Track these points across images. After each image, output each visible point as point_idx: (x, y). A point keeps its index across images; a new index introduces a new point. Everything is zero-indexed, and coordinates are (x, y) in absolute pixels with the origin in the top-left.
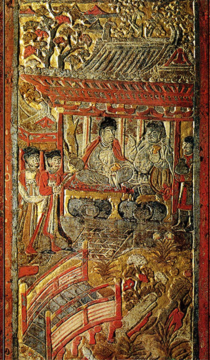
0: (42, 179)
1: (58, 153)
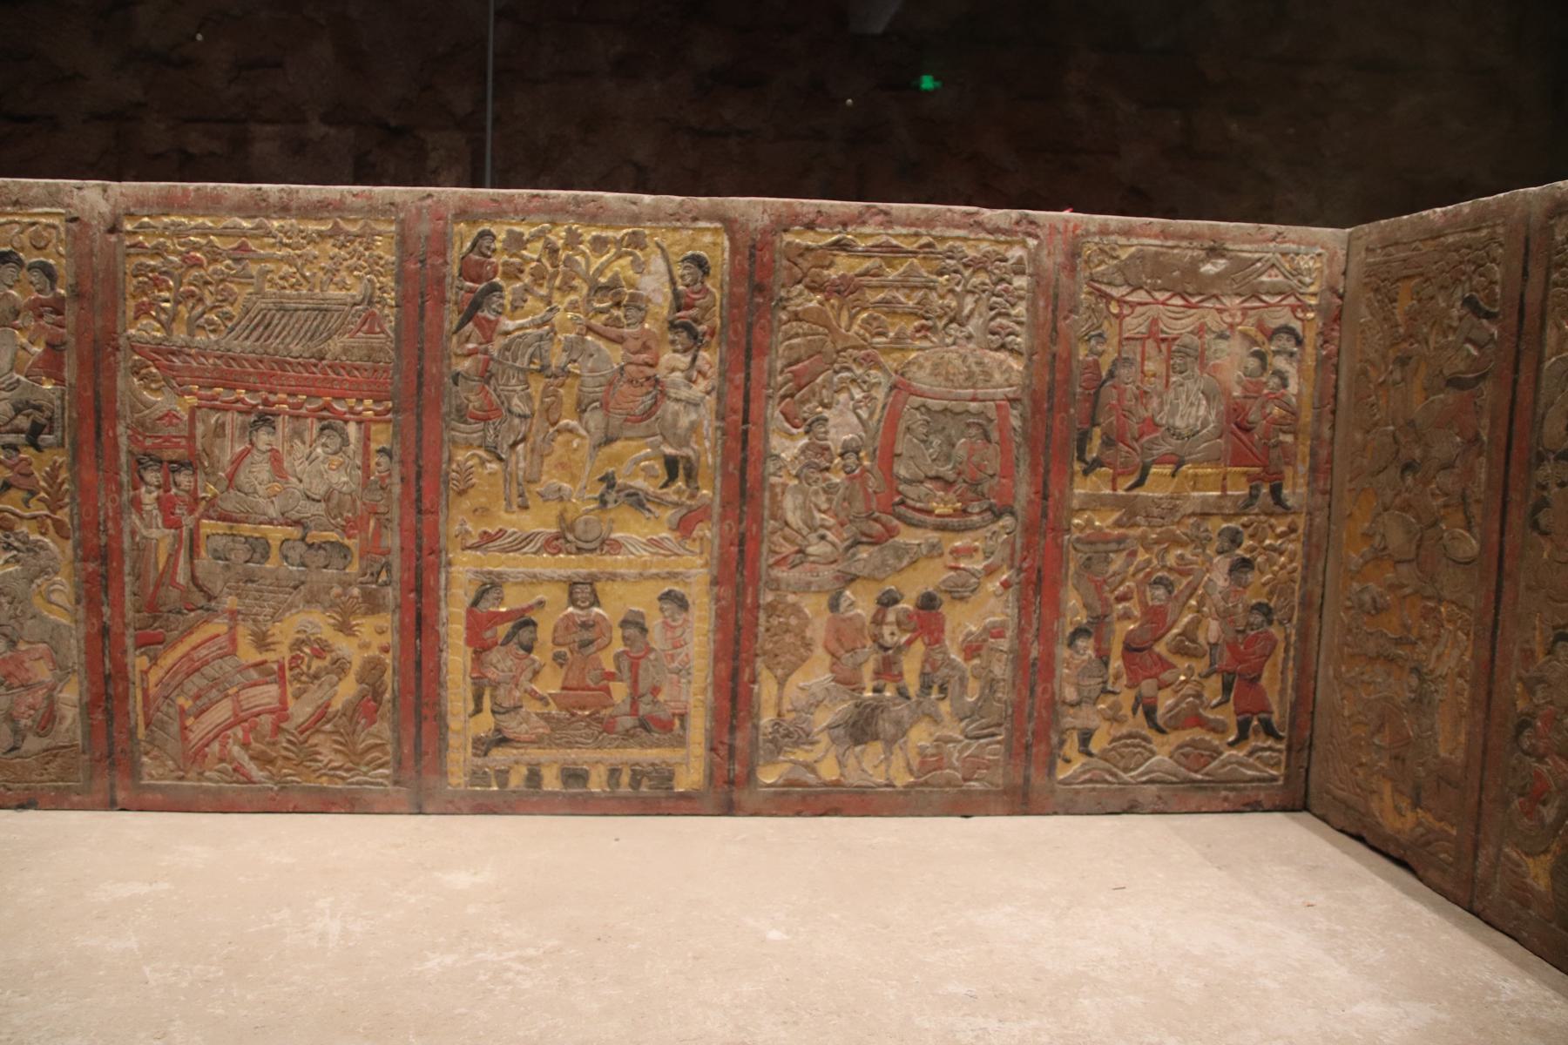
0: (166, 505)
1: (189, 464)
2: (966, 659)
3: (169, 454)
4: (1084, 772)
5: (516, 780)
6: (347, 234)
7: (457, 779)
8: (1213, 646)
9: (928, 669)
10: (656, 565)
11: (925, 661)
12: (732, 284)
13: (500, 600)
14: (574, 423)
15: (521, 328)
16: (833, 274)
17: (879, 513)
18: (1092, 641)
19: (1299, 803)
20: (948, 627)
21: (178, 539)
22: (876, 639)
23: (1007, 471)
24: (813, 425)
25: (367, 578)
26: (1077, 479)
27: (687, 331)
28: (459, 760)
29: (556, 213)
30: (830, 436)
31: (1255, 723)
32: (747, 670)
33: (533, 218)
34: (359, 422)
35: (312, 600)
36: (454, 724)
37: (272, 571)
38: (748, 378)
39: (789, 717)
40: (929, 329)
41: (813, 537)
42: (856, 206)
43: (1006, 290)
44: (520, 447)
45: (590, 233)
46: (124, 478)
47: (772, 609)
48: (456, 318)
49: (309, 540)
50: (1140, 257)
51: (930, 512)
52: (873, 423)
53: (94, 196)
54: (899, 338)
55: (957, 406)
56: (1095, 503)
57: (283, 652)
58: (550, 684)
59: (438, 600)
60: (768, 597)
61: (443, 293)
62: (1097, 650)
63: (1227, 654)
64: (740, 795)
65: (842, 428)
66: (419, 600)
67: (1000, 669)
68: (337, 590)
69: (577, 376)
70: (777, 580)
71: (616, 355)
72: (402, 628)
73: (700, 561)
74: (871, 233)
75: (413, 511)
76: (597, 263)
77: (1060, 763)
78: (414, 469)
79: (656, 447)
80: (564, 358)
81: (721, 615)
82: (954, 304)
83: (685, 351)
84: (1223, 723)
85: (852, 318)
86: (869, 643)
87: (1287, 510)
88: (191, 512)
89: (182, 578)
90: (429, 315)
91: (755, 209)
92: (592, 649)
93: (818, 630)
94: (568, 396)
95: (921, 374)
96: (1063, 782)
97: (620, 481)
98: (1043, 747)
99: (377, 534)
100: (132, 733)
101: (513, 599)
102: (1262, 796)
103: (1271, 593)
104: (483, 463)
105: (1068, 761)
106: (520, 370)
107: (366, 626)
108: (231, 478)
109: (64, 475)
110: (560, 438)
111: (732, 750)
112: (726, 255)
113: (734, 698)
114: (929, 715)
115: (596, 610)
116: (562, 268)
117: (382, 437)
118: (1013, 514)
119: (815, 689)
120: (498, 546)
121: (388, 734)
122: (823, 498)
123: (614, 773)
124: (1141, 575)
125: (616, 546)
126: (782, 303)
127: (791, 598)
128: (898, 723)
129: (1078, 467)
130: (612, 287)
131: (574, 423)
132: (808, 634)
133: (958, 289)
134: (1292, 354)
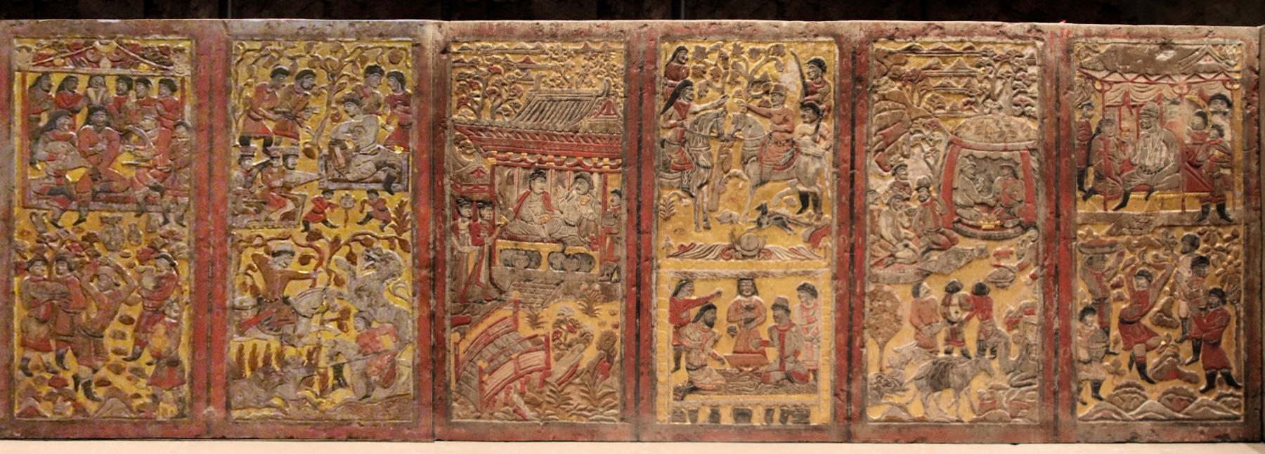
1: (490, 203)
2: (1009, 330)
3: (477, 196)
4: (1097, 412)
5: (703, 417)
6: (593, 51)
7: (663, 416)
8: (1184, 320)
9: (982, 337)
10: (795, 265)
11: (980, 332)
12: (841, 77)
13: (692, 291)
14: (739, 171)
15: (704, 109)
16: (907, 69)
17: (944, 230)
18: (1096, 316)
19: (1257, 437)
20: (995, 307)
21: (482, 253)
22: (945, 316)
23: (1031, 198)
24: (897, 170)
25: (605, 277)
26: (1080, 203)
27: (812, 109)
28: (665, 402)
29: (726, 34)
30: (910, 176)
31: (1219, 376)
32: (858, 339)
33: (712, 38)
34: (600, 173)
35: (568, 293)
36: (661, 377)
37: (542, 274)
38: (853, 139)
39: (888, 372)
40: (973, 103)
41: (900, 246)
42: (920, 24)
43: (1023, 76)
44: (705, 188)
45: (747, 47)
46: (448, 212)
47: (874, 296)
48: (663, 104)
49: (567, 252)
50: (1114, 51)
51: (979, 227)
52: (937, 167)
53: (431, 30)
54: (952, 110)
55: (994, 155)
56: (1093, 219)
57: (548, 329)
58: (725, 349)
59: (651, 293)
60: (871, 288)
61: (654, 87)
62: (1101, 323)
63: (1194, 326)
64: (856, 428)
65: (917, 171)
66: (638, 292)
67: (1033, 337)
68: (585, 286)
69: (742, 140)
70: (876, 276)
71: (766, 126)
72: (627, 312)
73: (824, 263)
74: (933, 41)
75: (635, 232)
76: (753, 66)
77: (1079, 404)
78: (635, 204)
79: (793, 186)
80: (733, 128)
81: (839, 300)
82: (989, 86)
83: (811, 122)
84: (1196, 377)
85: (921, 97)
86: (941, 319)
87: (1230, 222)
88: (490, 234)
89: (483, 279)
90: (645, 102)
91: (855, 28)
92: (753, 324)
93: (906, 309)
94: (735, 153)
95: (968, 134)
96: (1081, 419)
97: (770, 210)
98: (1066, 393)
99: (612, 248)
100: (447, 386)
101: (700, 291)
102: (1229, 430)
103: (1223, 281)
104: (680, 198)
105: (1085, 404)
106: (704, 137)
107: (604, 310)
108: (517, 211)
109: (408, 209)
110: (731, 182)
111: (849, 395)
112: (837, 58)
113: (850, 358)
114: (985, 370)
115: (755, 297)
116: (730, 70)
117: (615, 183)
118: (1036, 227)
119: (904, 352)
120: (692, 255)
121: (617, 385)
122: (906, 218)
123: (769, 411)
124: (1128, 270)
125: (769, 253)
126: (874, 89)
127: (886, 288)
128: (963, 376)
129: (1079, 194)
130: (763, 81)
131: (739, 171)
132: (899, 313)
133: (991, 76)
134: (1225, 114)
